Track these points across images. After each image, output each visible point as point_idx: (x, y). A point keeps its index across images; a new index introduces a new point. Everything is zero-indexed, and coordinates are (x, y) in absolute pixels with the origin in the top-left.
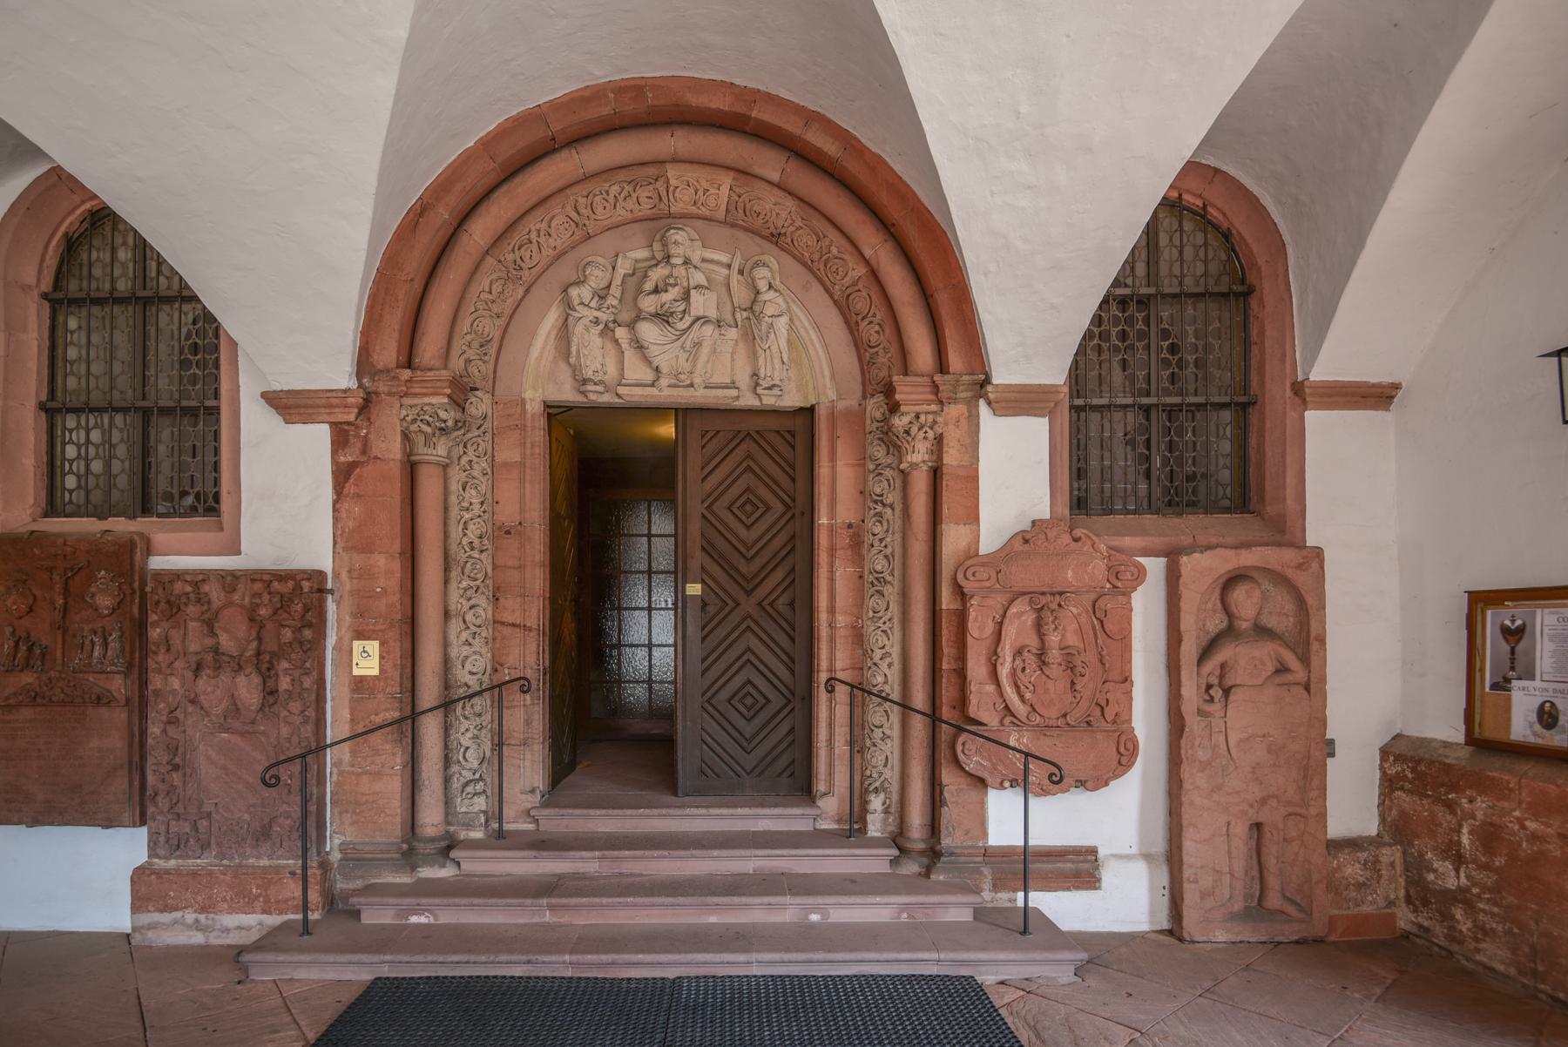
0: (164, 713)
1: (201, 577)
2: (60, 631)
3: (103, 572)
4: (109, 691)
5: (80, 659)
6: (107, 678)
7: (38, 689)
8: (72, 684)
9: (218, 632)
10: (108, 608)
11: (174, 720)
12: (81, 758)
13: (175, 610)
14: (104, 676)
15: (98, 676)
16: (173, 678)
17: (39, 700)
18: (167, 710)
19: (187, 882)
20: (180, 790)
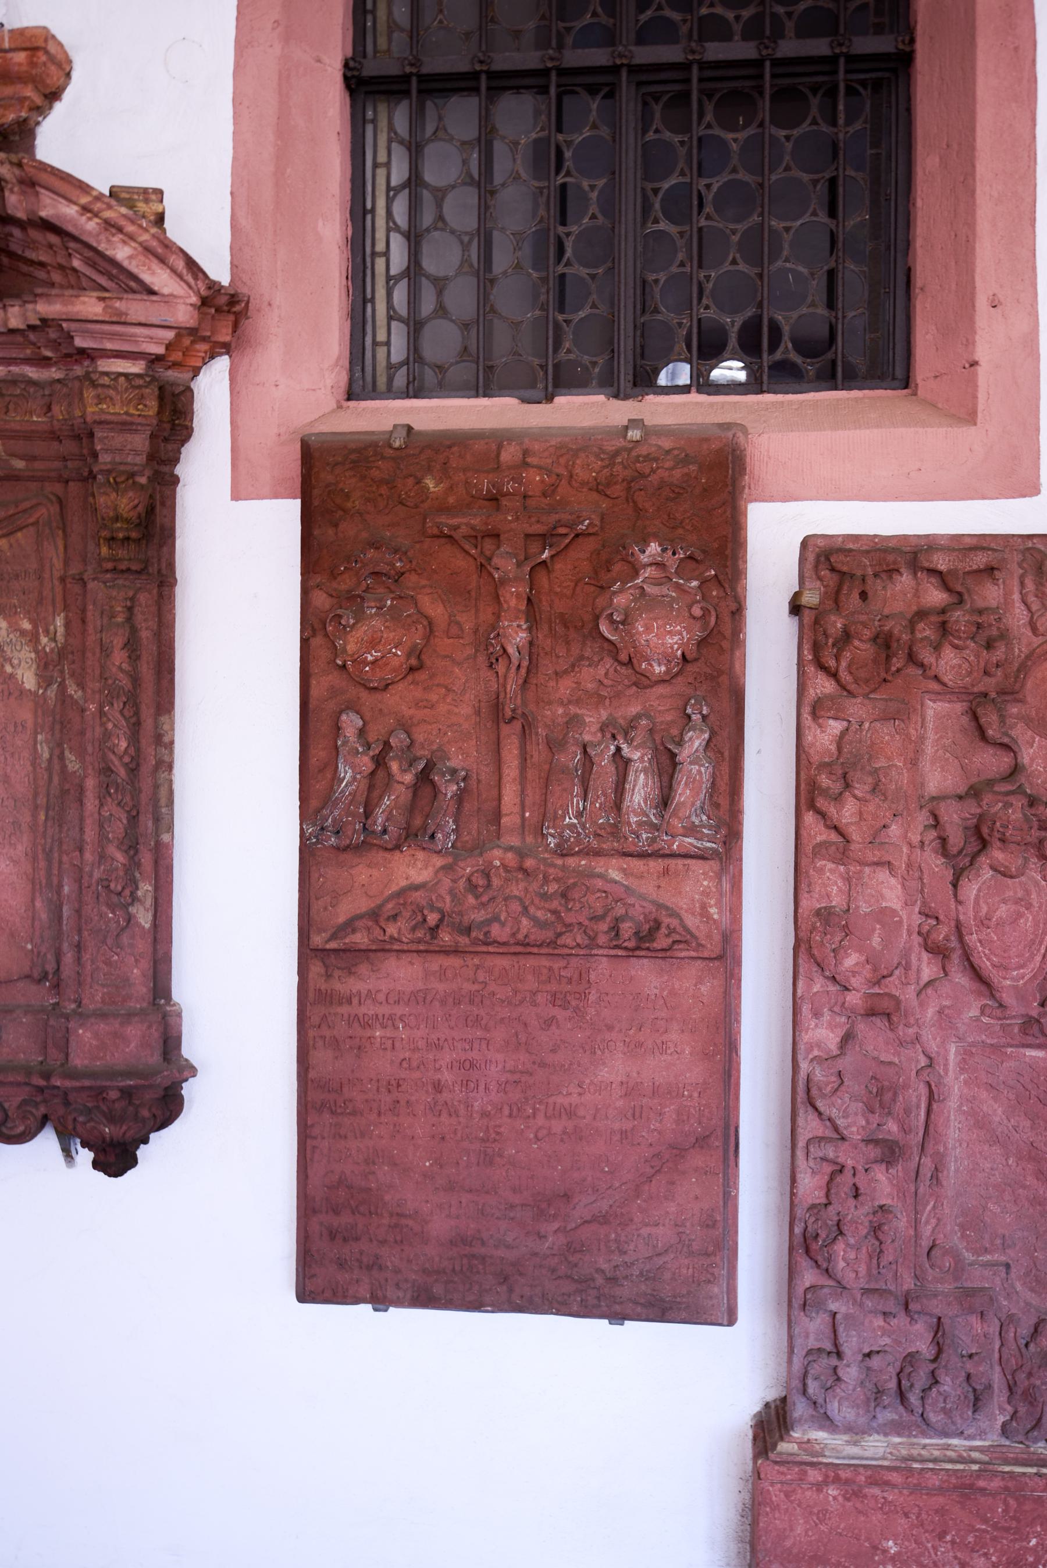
0: (855, 982)
1: (980, 560)
2: (517, 725)
3: (654, 548)
4: (674, 914)
5: (579, 815)
6: (666, 872)
7: (448, 904)
8: (553, 888)
9: (1020, 732)
10: (668, 659)
11: (886, 1004)
12: (571, 1113)
13: (897, 663)
14: (656, 865)
15: (637, 864)
16: (883, 875)
17: (446, 937)
18: (867, 971)
19: (941, 1511)
20: (901, 1223)
